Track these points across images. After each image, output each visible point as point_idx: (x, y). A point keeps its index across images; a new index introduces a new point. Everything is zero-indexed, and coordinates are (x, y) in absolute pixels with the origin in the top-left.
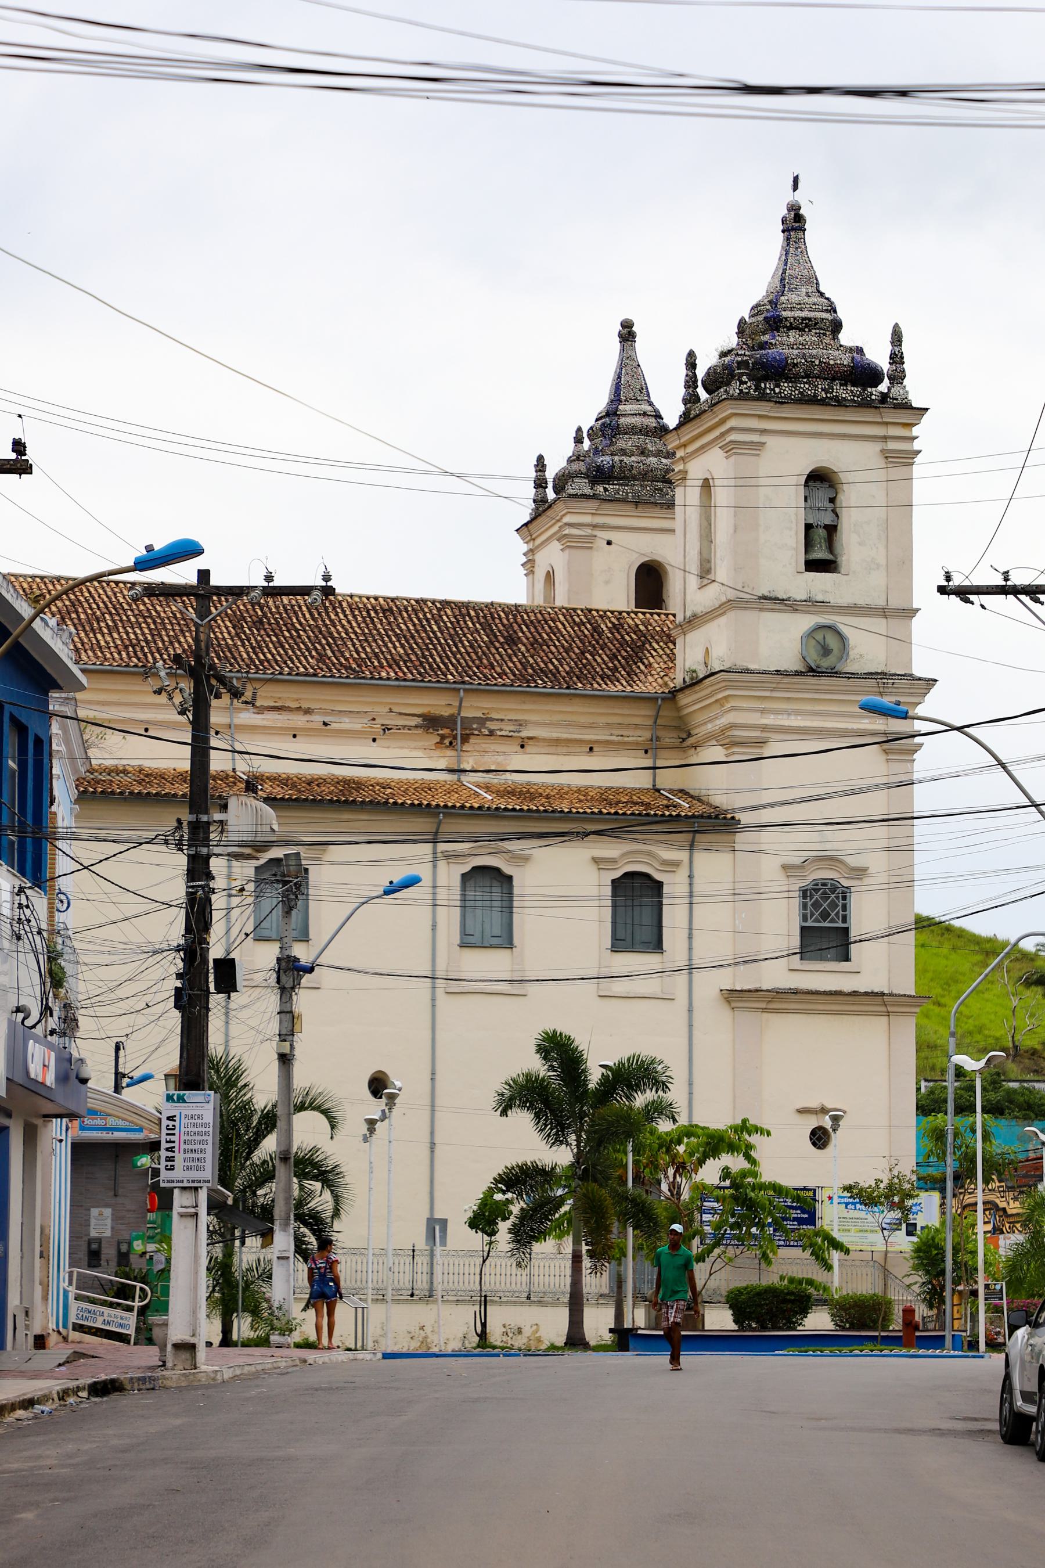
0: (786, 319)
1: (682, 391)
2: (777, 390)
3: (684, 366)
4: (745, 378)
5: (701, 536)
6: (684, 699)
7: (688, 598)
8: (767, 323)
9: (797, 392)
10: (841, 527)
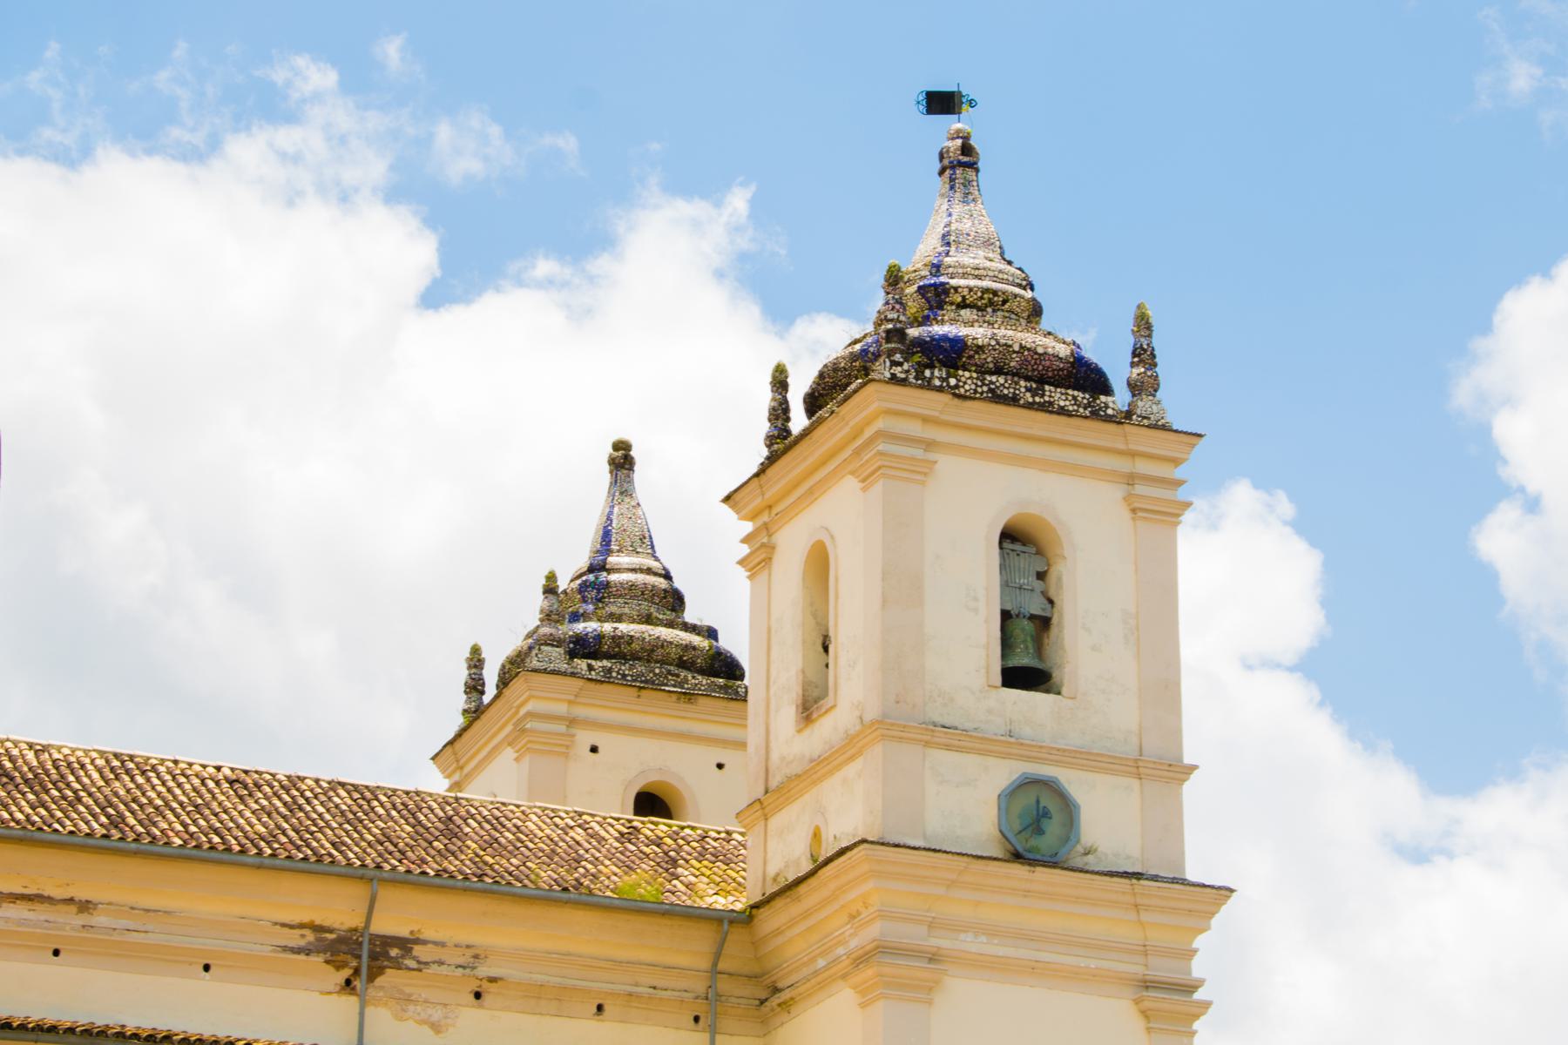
0: (956, 289)
1: (764, 427)
2: (953, 381)
3: (769, 387)
4: (898, 357)
8: (923, 296)
9: (985, 389)
10: (1061, 616)
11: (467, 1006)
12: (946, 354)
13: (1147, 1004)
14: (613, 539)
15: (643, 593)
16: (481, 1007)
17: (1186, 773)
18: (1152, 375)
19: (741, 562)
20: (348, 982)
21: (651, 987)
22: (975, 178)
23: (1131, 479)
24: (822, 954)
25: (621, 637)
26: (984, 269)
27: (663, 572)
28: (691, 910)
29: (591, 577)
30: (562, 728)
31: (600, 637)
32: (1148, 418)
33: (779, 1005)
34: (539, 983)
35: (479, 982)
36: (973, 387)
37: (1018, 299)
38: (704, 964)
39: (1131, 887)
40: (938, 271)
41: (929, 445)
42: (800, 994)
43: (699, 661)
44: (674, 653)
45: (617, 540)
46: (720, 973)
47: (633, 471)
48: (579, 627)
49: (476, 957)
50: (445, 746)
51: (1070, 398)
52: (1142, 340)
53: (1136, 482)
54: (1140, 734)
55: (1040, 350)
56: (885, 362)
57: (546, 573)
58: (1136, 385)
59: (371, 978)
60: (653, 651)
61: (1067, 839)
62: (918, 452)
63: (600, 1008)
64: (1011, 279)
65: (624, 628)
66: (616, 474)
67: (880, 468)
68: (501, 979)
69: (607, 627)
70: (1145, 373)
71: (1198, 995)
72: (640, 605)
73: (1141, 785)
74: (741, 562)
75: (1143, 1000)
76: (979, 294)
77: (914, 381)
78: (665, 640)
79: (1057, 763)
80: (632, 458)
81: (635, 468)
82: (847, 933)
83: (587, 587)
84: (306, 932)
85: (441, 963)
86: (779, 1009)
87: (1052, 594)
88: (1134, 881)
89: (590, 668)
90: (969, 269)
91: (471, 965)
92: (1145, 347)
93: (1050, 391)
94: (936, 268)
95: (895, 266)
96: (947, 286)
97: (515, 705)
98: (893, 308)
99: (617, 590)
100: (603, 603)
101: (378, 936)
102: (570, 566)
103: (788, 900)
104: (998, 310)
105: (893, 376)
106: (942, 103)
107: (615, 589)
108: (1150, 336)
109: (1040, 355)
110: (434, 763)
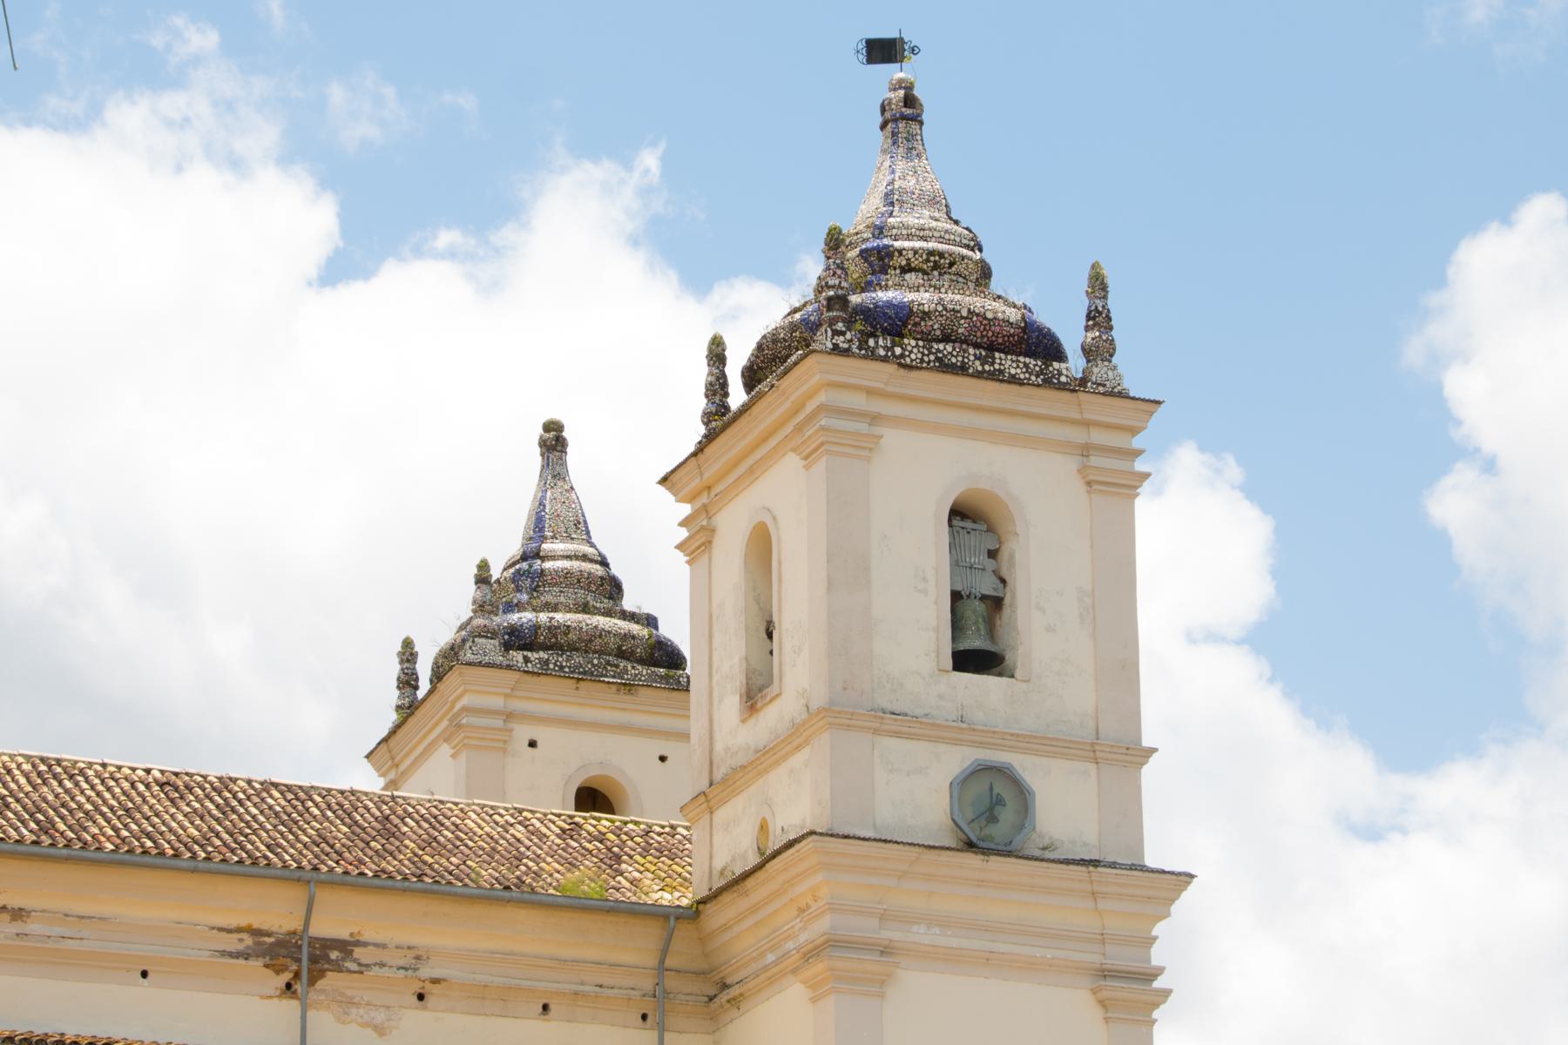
0: (900, 252)
2: (898, 351)
4: (840, 326)
5: (747, 628)
6: (716, 916)
7: (719, 747)
8: (866, 260)
9: (932, 357)
11: (410, 1008)
12: (891, 322)
13: (1105, 994)
14: (547, 526)
15: (579, 581)
16: (425, 1008)
17: (1145, 757)
18: (1108, 339)
19: (680, 547)
20: (289, 986)
21: (597, 986)
22: (919, 132)
23: (1086, 450)
24: (771, 949)
25: (556, 628)
26: (930, 229)
27: (599, 559)
28: (636, 907)
29: (525, 565)
30: (499, 723)
31: (536, 627)
32: (1104, 386)
33: (728, 1001)
34: (483, 984)
35: (421, 984)
36: (919, 356)
37: (966, 261)
38: (651, 960)
39: (1087, 875)
40: (881, 232)
41: (875, 419)
42: (750, 990)
43: (639, 650)
44: (612, 643)
45: (550, 526)
46: (667, 970)
47: (566, 453)
48: (514, 617)
49: (418, 958)
50: (379, 744)
51: (1021, 365)
52: (1098, 301)
53: (1091, 453)
54: (1097, 718)
55: (989, 315)
56: (826, 331)
57: (478, 562)
58: (1091, 350)
59: (312, 981)
60: (591, 641)
61: (1021, 827)
62: (863, 427)
63: (545, 1007)
64: (958, 239)
65: (560, 617)
66: (548, 457)
67: (822, 444)
68: (444, 980)
69: (543, 617)
70: (1100, 336)
71: (1156, 984)
72: (576, 593)
73: (1098, 768)
74: (680, 547)
75: (1101, 990)
76: (925, 257)
77: (858, 351)
78: (603, 630)
79: (1012, 749)
80: (564, 439)
81: (568, 450)
82: (797, 928)
83: (522, 575)
84: (244, 936)
85: (382, 965)
86: (729, 1005)
87: (1004, 573)
88: (1091, 868)
89: (526, 660)
90: (913, 230)
91: (413, 966)
92: (1101, 309)
93: (1000, 359)
94: (879, 231)
95: (835, 229)
96: (891, 249)
97: (450, 699)
98: (834, 274)
99: (552, 579)
100: (538, 592)
101: (316, 939)
102: (503, 550)
103: (735, 895)
104: (945, 273)
105: (836, 346)
106: (883, 51)
107: (550, 577)
108: (1105, 297)
109: (989, 320)
110: (369, 762)
